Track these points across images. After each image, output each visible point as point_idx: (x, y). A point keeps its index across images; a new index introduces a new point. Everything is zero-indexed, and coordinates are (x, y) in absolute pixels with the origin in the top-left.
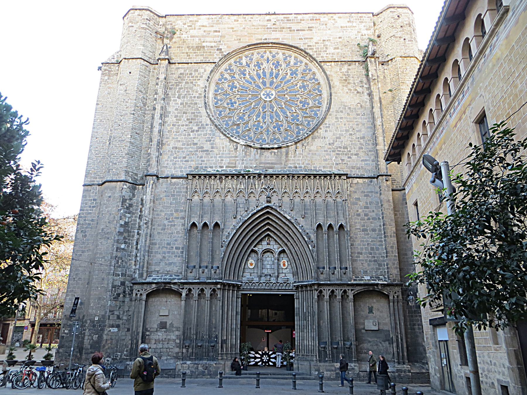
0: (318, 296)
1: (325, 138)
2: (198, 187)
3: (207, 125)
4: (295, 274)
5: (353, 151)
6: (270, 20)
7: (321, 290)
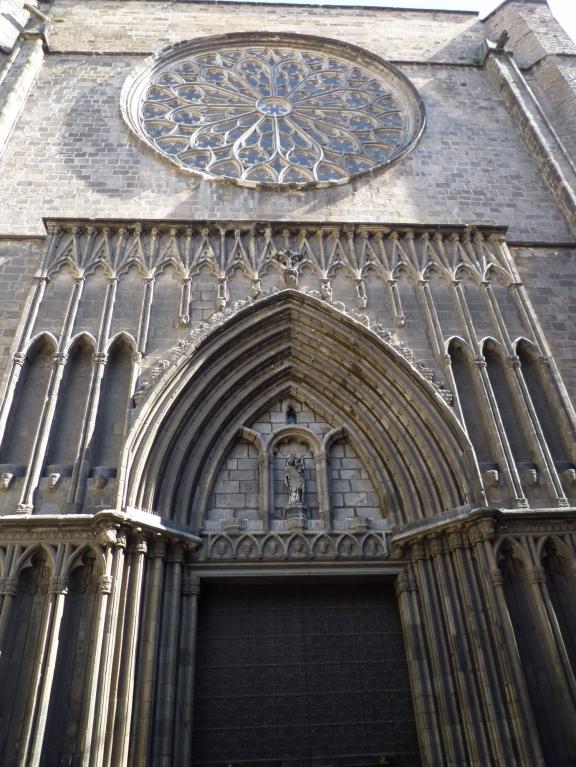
0: (501, 565)
1: (423, 174)
2: (75, 252)
3: (120, 145)
4: (391, 504)
5: (505, 199)
6: (274, 12)
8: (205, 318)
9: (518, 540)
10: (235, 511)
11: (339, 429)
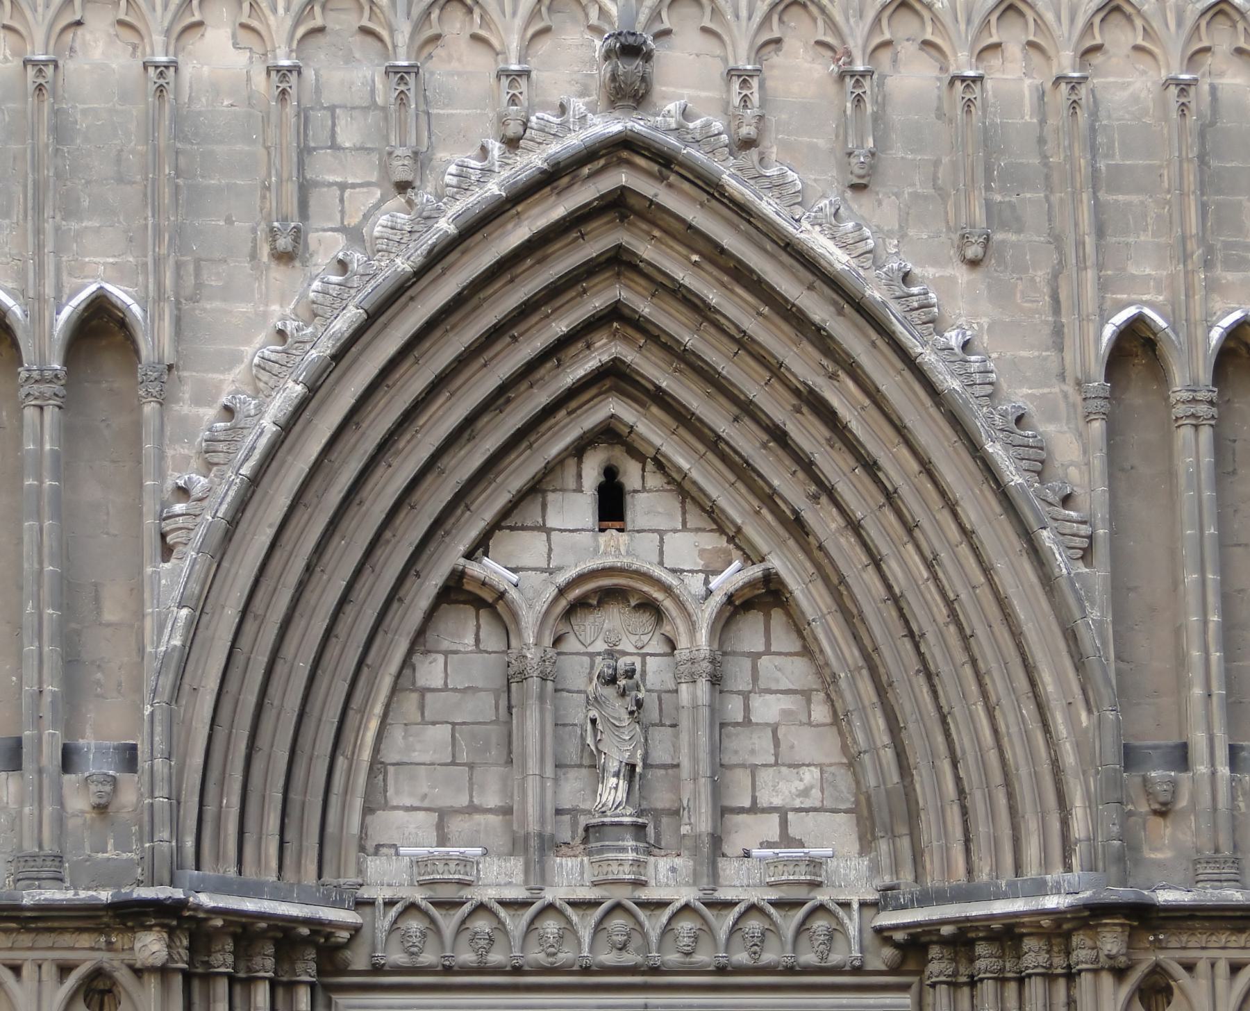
7: (1158, 970)
8: (353, 220)
9: (1189, 967)
10: (443, 815)
11: (755, 571)
